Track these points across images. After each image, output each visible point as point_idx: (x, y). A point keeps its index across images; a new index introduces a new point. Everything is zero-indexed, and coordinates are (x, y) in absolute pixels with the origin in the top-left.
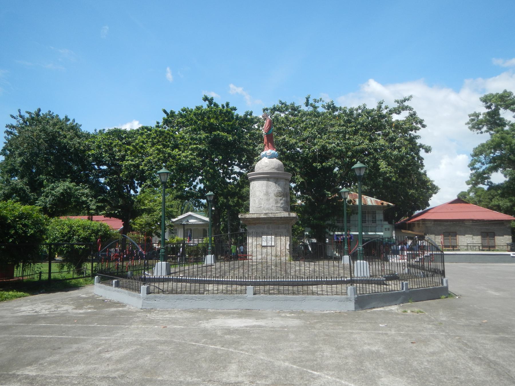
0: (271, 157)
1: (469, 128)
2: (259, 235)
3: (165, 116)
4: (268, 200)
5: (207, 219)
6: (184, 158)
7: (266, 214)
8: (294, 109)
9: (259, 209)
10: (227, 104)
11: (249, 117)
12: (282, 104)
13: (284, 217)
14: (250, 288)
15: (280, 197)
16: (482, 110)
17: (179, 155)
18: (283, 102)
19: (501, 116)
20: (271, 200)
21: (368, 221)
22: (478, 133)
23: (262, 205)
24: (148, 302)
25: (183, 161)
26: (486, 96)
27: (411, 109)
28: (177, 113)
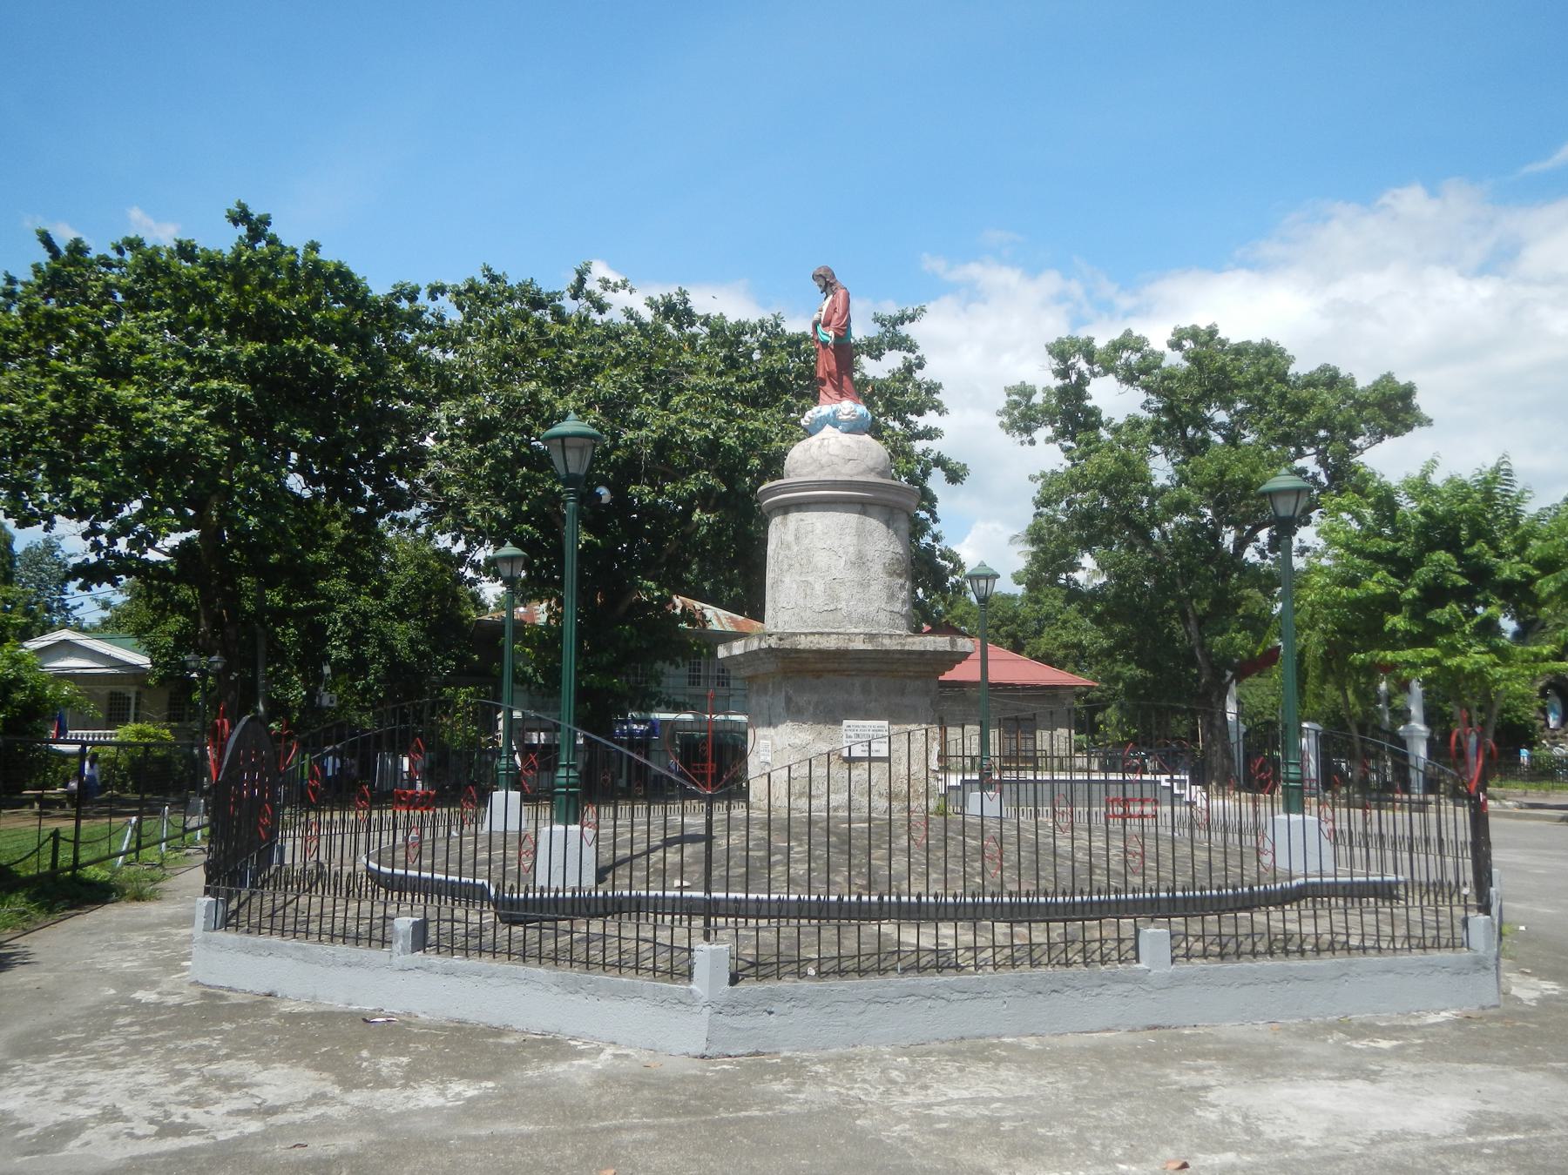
0: (854, 428)
1: (1002, 425)
2: (831, 715)
3: (43, 257)
4: (864, 585)
5: (143, 660)
6: (166, 424)
7: (871, 637)
8: (537, 303)
9: (831, 616)
10: (314, 247)
11: (404, 305)
12: (494, 279)
13: (935, 652)
14: (1155, 935)
15: (900, 576)
16: (1042, 377)
17: (144, 409)
18: (497, 272)
19: (1089, 403)
20: (877, 589)
21: (707, 677)
22: (1022, 443)
23: (842, 605)
24: (728, 1020)
25: (164, 432)
26: (1060, 342)
27: (911, 348)
28: (92, 255)
